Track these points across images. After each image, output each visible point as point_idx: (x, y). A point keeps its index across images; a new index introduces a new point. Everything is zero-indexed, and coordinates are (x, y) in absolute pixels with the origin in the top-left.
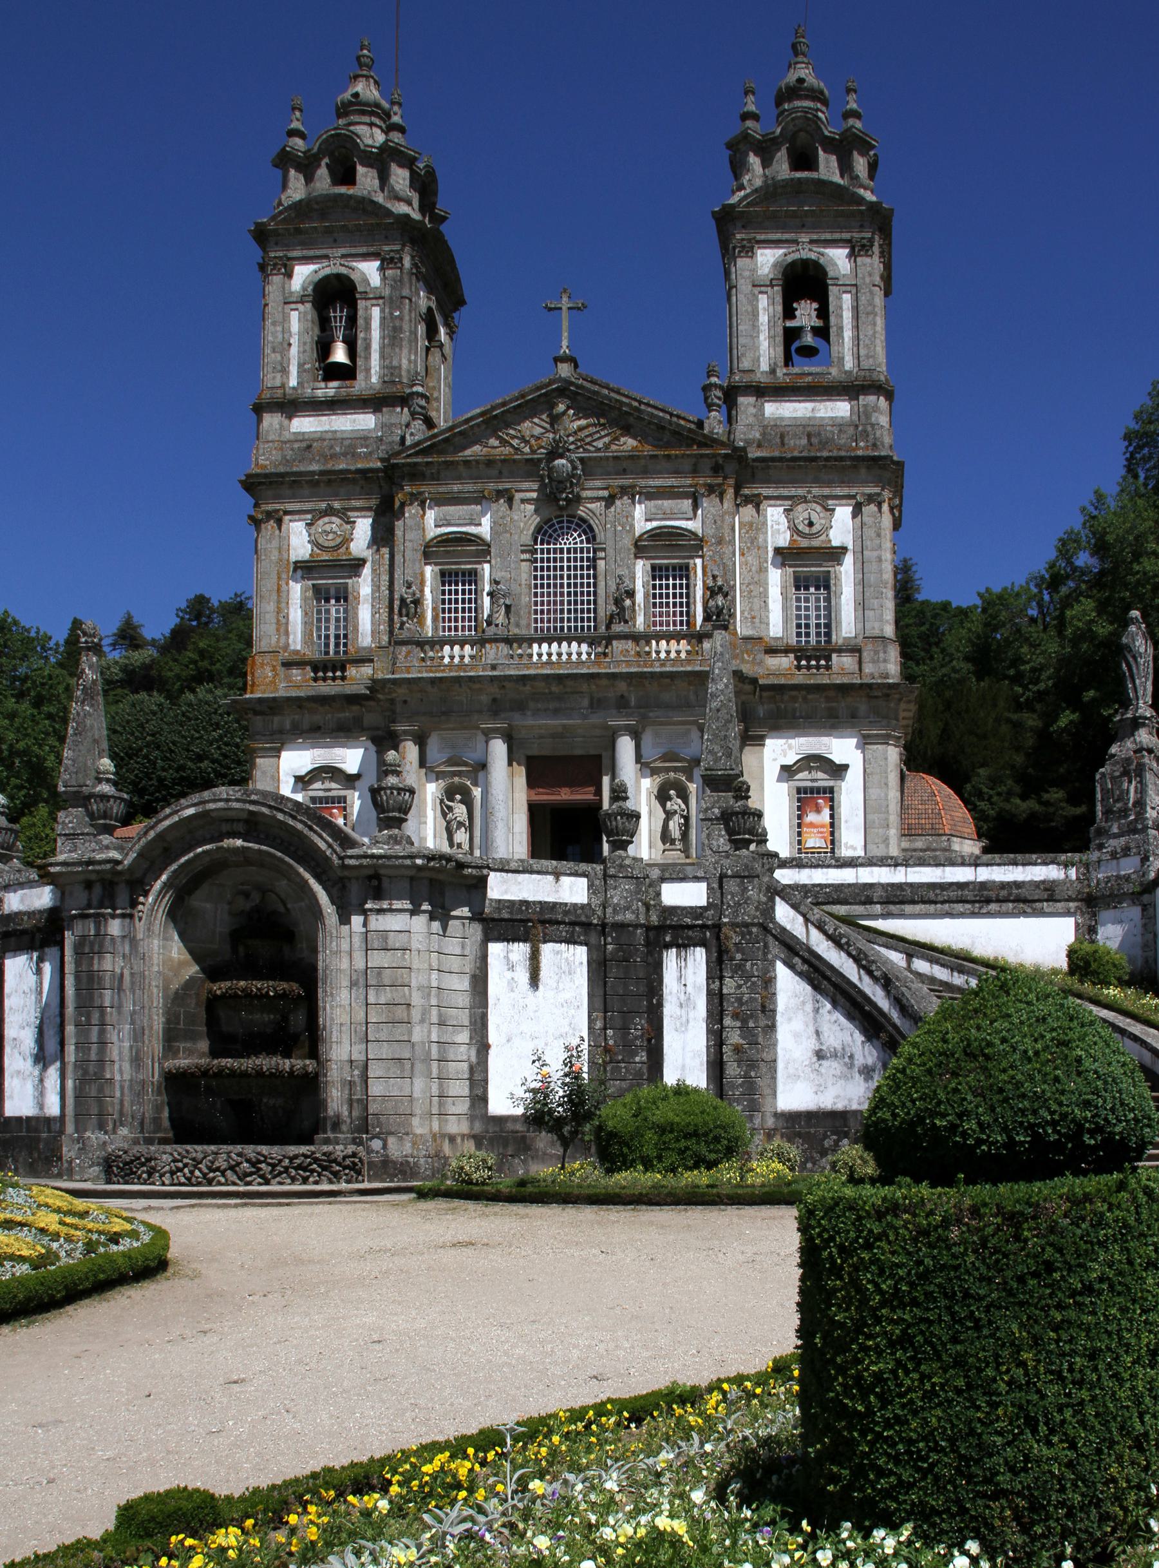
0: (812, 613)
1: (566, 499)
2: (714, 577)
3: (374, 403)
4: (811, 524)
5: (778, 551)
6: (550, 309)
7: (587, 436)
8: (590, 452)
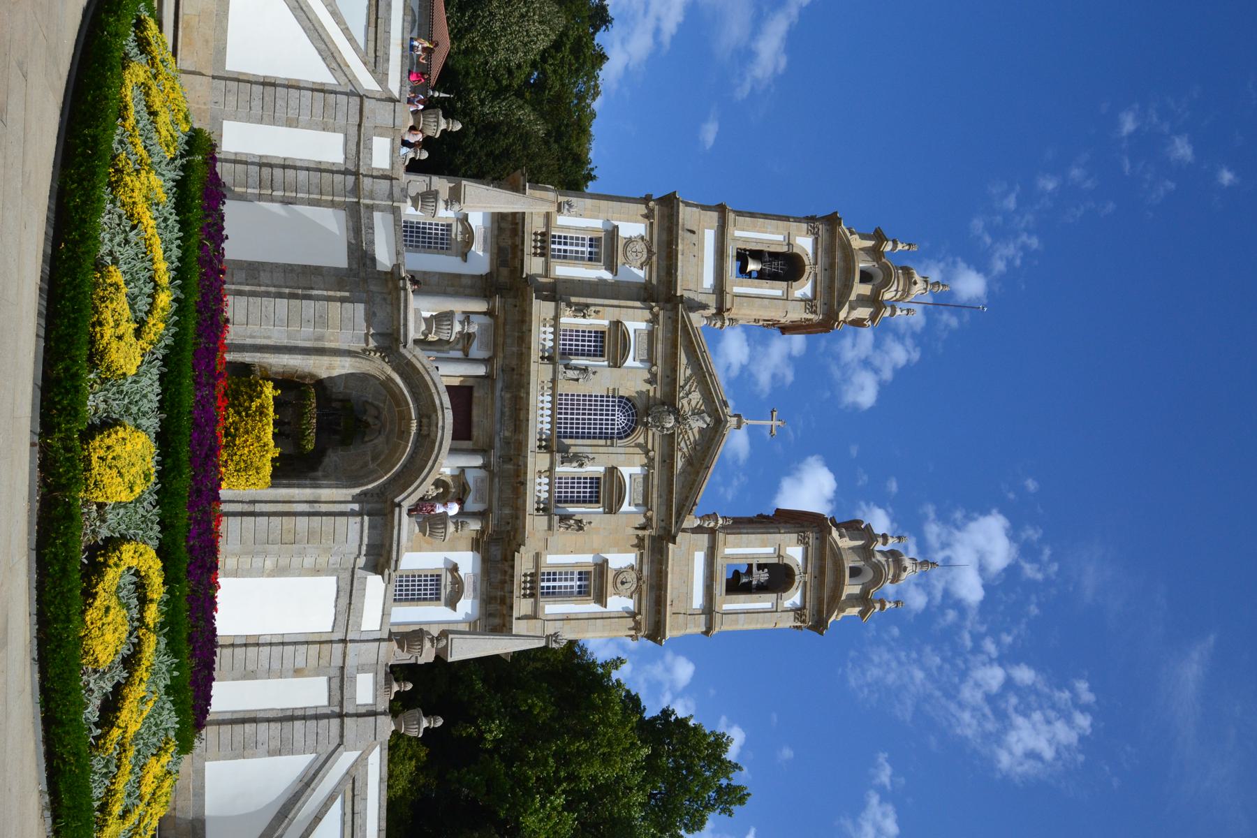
0: (563, 584)
1: (647, 422)
2: (590, 523)
3: (719, 289)
4: (623, 583)
5: (606, 561)
6: (772, 412)
7: (688, 436)
8: (678, 438)
